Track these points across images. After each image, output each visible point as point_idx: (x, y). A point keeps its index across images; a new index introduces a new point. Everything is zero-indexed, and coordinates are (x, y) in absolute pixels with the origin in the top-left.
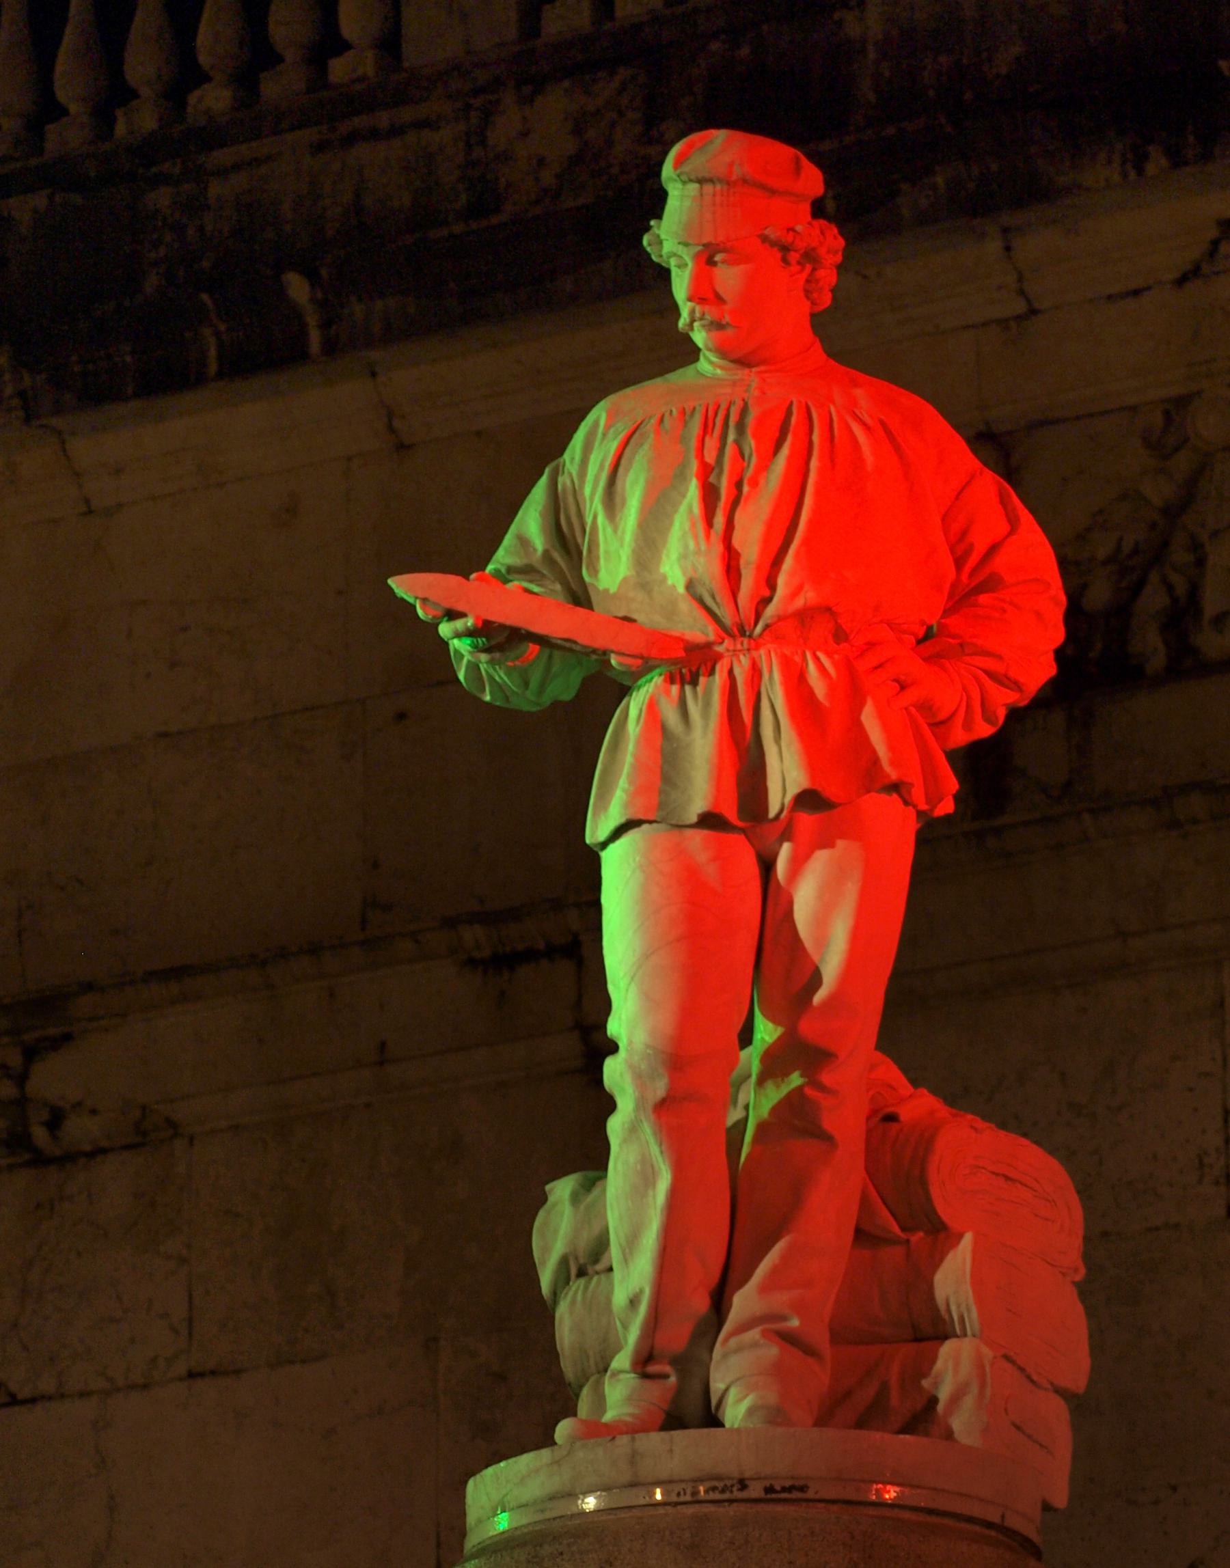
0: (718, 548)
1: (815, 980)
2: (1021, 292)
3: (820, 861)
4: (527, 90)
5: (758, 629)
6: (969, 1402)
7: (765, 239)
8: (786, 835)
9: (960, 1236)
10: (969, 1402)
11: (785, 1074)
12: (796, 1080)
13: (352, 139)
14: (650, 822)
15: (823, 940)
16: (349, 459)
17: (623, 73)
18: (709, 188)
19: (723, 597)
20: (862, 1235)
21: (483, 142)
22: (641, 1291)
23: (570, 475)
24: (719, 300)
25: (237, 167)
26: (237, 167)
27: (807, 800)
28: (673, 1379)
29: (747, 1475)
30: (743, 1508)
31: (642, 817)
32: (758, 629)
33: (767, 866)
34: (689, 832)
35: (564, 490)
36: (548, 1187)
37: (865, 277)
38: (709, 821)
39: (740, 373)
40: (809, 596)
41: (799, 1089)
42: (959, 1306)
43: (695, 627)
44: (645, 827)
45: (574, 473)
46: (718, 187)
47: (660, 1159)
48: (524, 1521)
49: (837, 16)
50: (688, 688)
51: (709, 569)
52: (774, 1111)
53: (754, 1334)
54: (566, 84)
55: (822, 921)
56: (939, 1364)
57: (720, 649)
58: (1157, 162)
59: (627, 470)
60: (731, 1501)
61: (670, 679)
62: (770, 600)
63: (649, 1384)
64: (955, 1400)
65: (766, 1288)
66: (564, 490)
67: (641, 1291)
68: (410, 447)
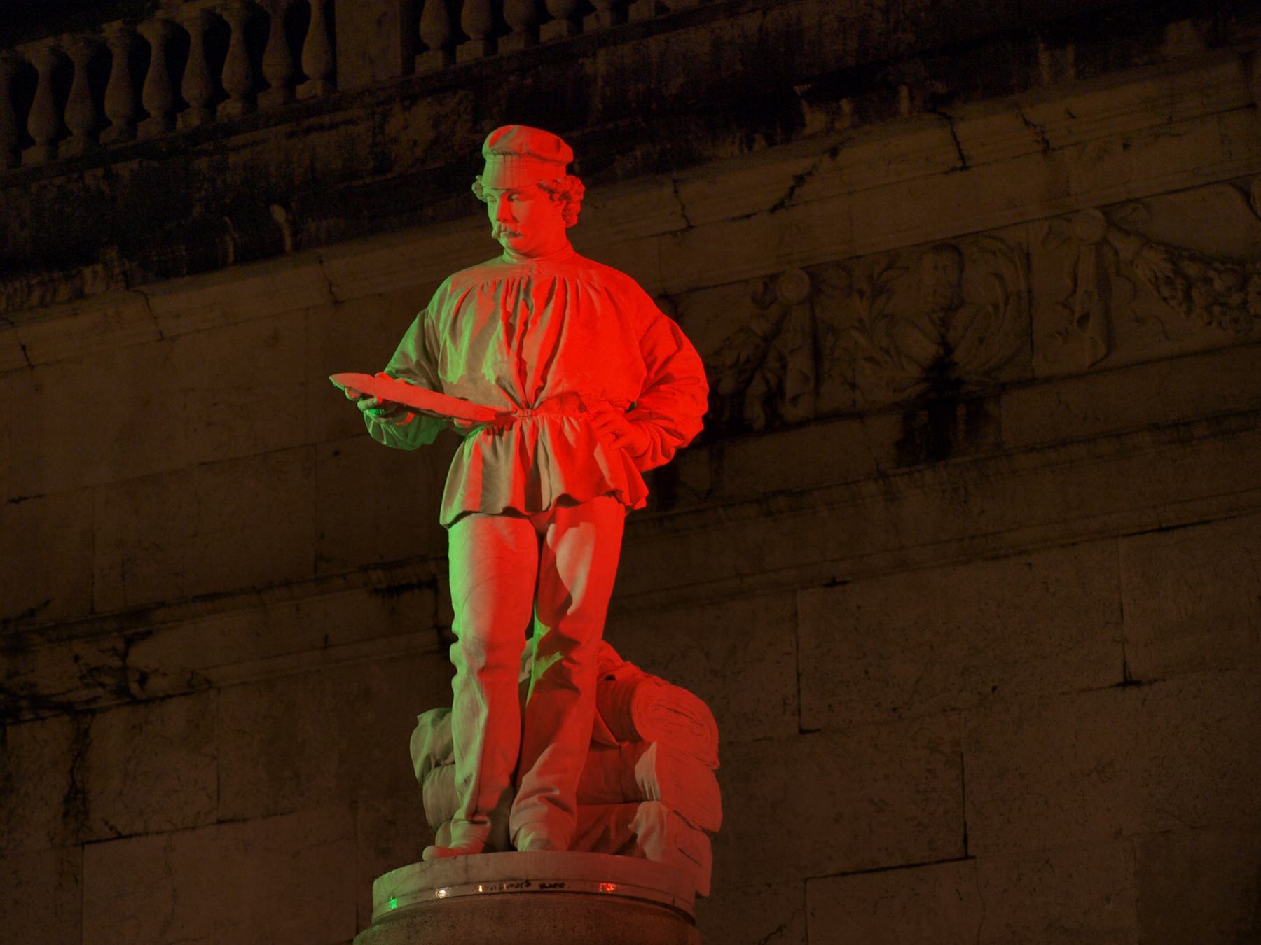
0: (514, 359)
1: (569, 601)
2: (684, 216)
3: (572, 533)
4: (407, 103)
5: (536, 405)
6: (654, 837)
7: (540, 186)
8: (552, 519)
9: (649, 744)
10: (654, 837)
11: (552, 653)
12: (557, 657)
13: (309, 130)
14: (476, 512)
15: (572, 579)
16: (308, 309)
17: (461, 93)
18: (509, 158)
19: (517, 386)
20: (594, 743)
22: (471, 775)
23: (431, 318)
24: (514, 220)
25: (244, 146)
26: (244, 146)
27: (564, 500)
28: (489, 824)
29: (530, 877)
30: (528, 896)
31: (470, 509)
32: (536, 405)
33: (541, 537)
34: (498, 518)
35: (428, 326)
36: (418, 717)
37: (596, 207)
38: (509, 512)
39: (527, 261)
40: (565, 386)
41: (560, 662)
42: (649, 783)
43: (501, 403)
44: (473, 515)
45: (433, 317)
46: (514, 157)
47: (481, 701)
48: (405, 904)
49: (580, 61)
50: (497, 438)
51: (509, 371)
52: (545, 674)
53: (534, 799)
54: (429, 99)
55: (572, 567)
56: (638, 815)
57: (515, 415)
58: (760, 143)
59: (463, 316)
60: (521, 892)
61: (487, 433)
62: (543, 388)
63: (475, 827)
64: (647, 836)
65: (540, 774)
66: (428, 326)
67: (471, 775)
68: (342, 302)
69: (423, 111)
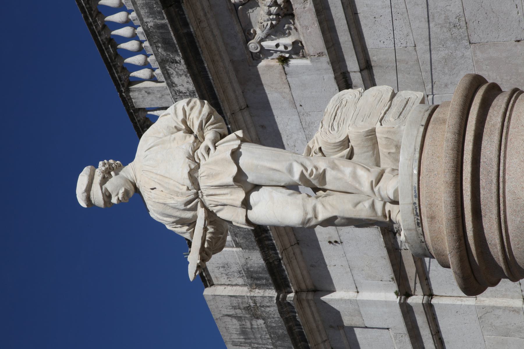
4: (174, 85)
16: (251, 116)
17: (168, 67)
21: (186, 93)
29: (412, 201)
37: (200, 22)
49: (150, 27)
54: (172, 78)
68: (247, 105)
69: (176, 80)
